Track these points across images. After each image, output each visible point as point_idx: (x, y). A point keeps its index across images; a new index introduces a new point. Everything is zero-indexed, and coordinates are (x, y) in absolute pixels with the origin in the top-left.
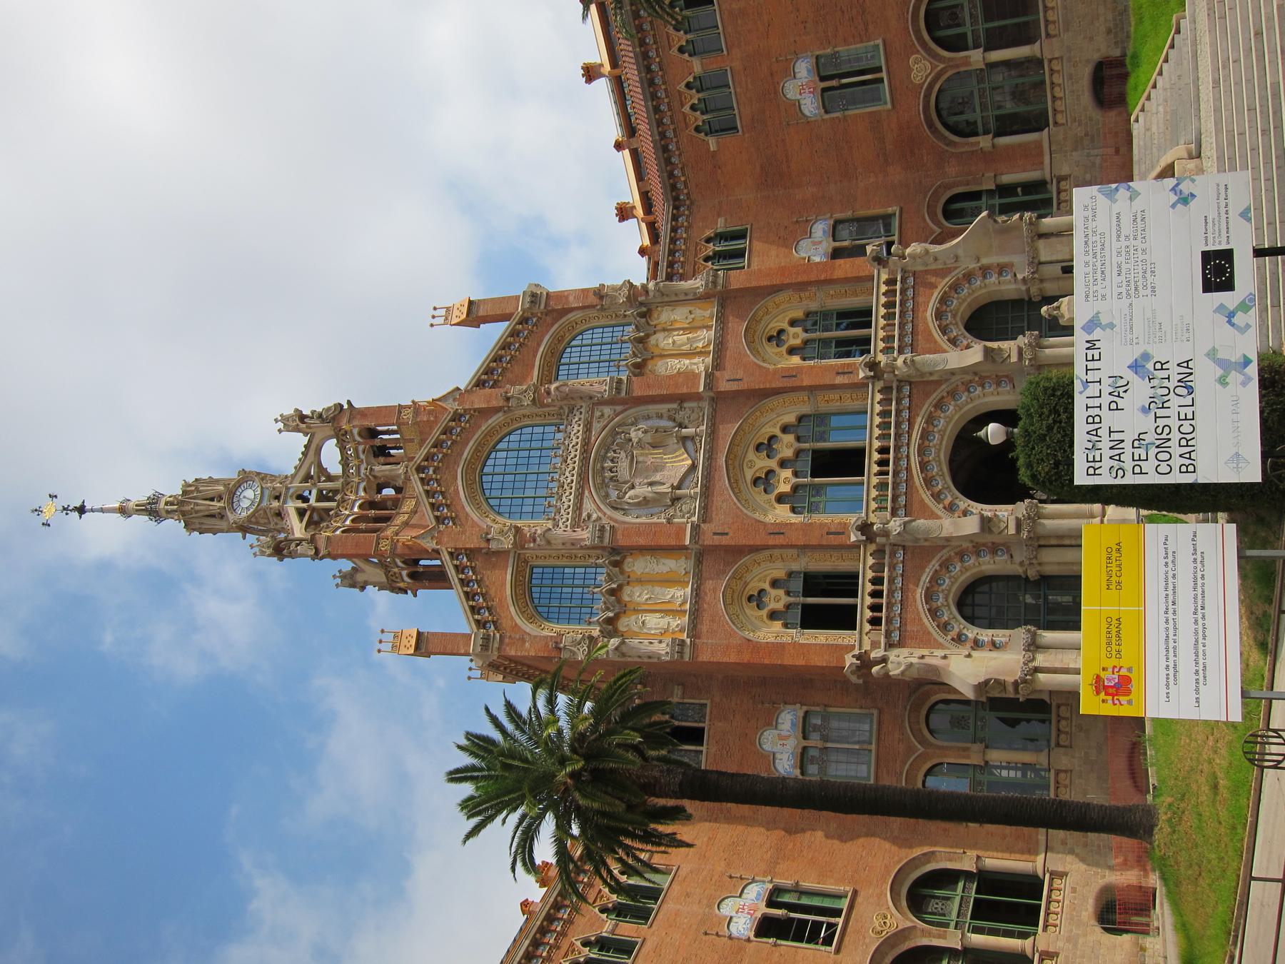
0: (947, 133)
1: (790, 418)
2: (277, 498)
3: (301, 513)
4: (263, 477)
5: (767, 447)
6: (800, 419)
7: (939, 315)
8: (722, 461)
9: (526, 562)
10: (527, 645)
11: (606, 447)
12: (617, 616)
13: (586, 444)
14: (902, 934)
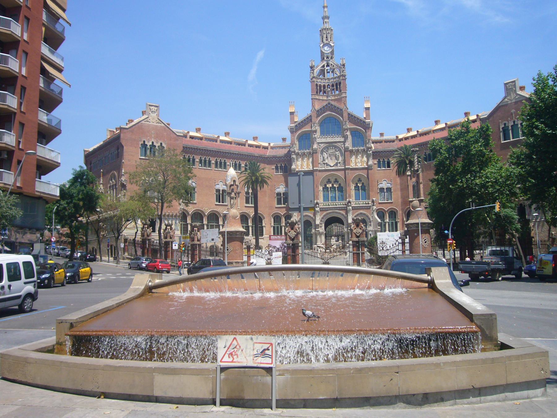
0: (408, 211)
1: (342, 185)
2: (327, 58)
3: (323, 66)
4: (332, 53)
5: (336, 181)
6: (342, 187)
7: (361, 213)
8: (332, 173)
9: (311, 132)
10: (293, 137)
11: (336, 147)
12: (300, 155)
13: (336, 142)
14: (249, 216)
